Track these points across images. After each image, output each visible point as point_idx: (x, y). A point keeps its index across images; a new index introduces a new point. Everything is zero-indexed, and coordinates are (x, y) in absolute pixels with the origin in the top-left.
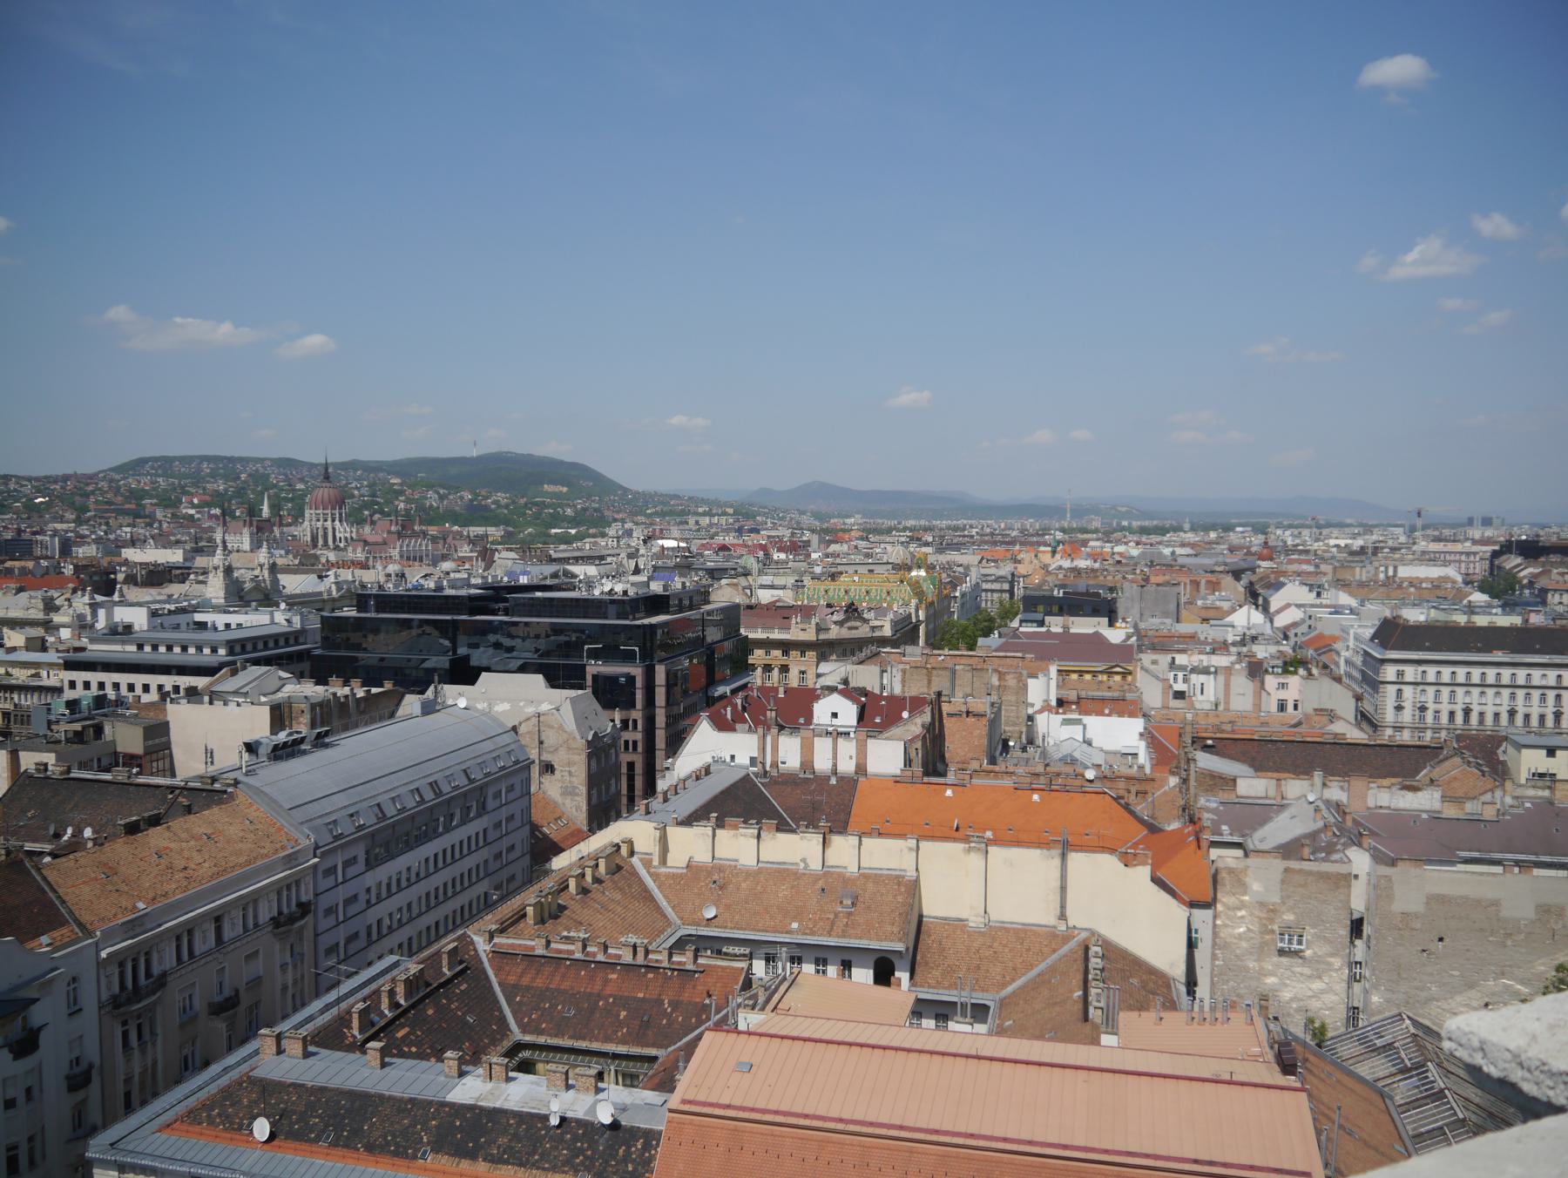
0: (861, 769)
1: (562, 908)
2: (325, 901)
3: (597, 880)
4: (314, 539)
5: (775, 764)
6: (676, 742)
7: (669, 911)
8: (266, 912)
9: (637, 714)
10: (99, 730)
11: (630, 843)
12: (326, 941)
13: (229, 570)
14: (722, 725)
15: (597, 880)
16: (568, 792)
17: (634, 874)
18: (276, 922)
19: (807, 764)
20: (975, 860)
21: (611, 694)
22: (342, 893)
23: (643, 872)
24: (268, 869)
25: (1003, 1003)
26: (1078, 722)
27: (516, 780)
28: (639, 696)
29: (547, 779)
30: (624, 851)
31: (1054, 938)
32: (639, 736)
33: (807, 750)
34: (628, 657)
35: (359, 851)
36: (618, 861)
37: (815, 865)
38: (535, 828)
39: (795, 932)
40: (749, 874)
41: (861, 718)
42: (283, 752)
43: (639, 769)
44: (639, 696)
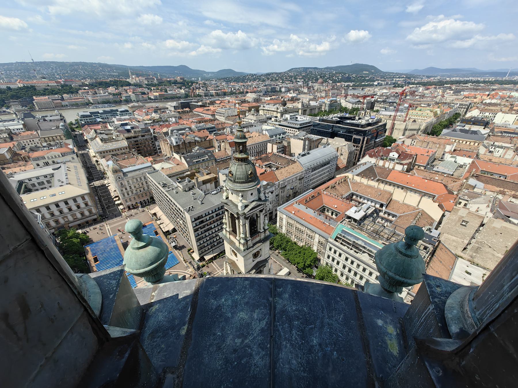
0: (393, 168)
1: (335, 186)
2: (305, 177)
3: (341, 182)
4: (317, 90)
5: (378, 164)
6: (363, 156)
7: (351, 188)
8: (298, 178)
9: (360, 145)
10: (282, 142)
11: (348, 176)
12: (305, 181)
13: (302, 102)
14: (371, 156)
15: (341, 182)
16: (344, 159)
17: (348, 181)
18: (299, 179)
19: (384, 166)
20: (405, 194)
21: (356, 141)
22: (308, 175)
23: (349, 181)
24: (299, 173)
25: (400, 216)
26: (455, 157)
27: (335, 159)
28: (361, 142)
29: (341, 156)
30: (347, 177)
31: (414, 209)
32: (359, 149)
33: (385, 163)
34: (361, 135)
35: (311, 170)
36: (345, 180)
37: (376, 187)
38: (337, 165)
39: (369, 197)
40: (365, 185)
41: (398, 157)
42: (303, 155)
43: (358, 154)
44: (361, 142)
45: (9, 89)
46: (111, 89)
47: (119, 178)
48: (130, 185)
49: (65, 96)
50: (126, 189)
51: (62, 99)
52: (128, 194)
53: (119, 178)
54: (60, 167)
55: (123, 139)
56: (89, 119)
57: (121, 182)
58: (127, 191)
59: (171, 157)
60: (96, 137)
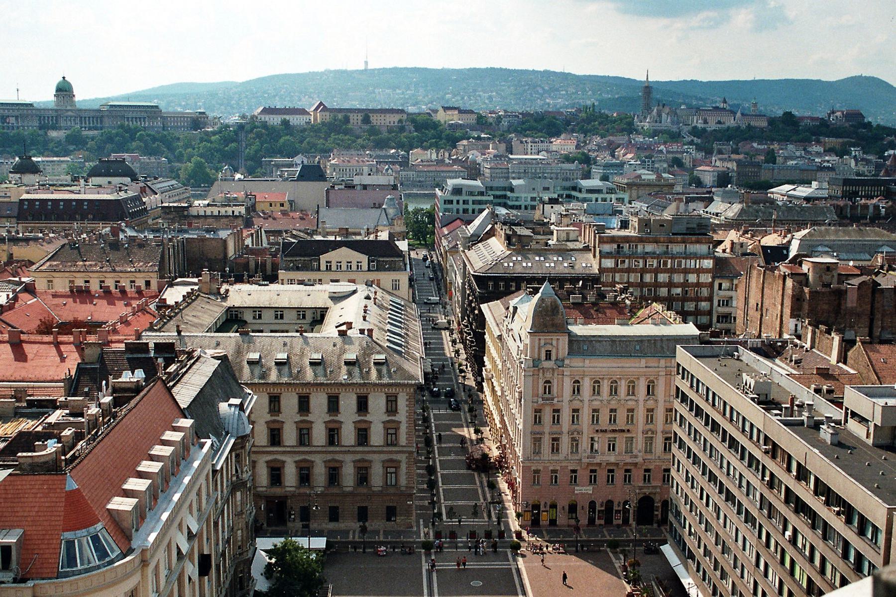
45: (285, 123)
46: (563, 144)
47: (548, 356)
48: (576, 404)
49: (417, 155)
50: (556, 420)
51: (405, 163)
52: (555, 449)
53: (548, 356)
54: (354, 292)
55: (586, 249)
56: (474, 202)
57: (548, 376)
58: (555, 428)
59: (785, 343)
60: (491, 234)
